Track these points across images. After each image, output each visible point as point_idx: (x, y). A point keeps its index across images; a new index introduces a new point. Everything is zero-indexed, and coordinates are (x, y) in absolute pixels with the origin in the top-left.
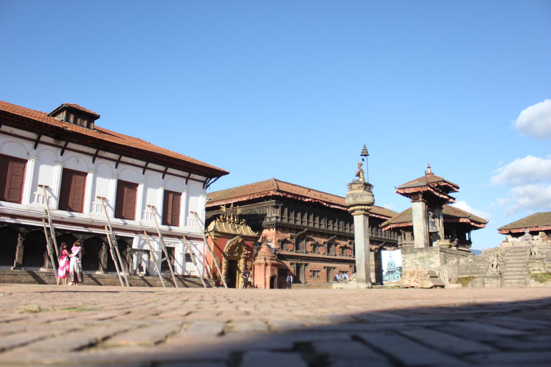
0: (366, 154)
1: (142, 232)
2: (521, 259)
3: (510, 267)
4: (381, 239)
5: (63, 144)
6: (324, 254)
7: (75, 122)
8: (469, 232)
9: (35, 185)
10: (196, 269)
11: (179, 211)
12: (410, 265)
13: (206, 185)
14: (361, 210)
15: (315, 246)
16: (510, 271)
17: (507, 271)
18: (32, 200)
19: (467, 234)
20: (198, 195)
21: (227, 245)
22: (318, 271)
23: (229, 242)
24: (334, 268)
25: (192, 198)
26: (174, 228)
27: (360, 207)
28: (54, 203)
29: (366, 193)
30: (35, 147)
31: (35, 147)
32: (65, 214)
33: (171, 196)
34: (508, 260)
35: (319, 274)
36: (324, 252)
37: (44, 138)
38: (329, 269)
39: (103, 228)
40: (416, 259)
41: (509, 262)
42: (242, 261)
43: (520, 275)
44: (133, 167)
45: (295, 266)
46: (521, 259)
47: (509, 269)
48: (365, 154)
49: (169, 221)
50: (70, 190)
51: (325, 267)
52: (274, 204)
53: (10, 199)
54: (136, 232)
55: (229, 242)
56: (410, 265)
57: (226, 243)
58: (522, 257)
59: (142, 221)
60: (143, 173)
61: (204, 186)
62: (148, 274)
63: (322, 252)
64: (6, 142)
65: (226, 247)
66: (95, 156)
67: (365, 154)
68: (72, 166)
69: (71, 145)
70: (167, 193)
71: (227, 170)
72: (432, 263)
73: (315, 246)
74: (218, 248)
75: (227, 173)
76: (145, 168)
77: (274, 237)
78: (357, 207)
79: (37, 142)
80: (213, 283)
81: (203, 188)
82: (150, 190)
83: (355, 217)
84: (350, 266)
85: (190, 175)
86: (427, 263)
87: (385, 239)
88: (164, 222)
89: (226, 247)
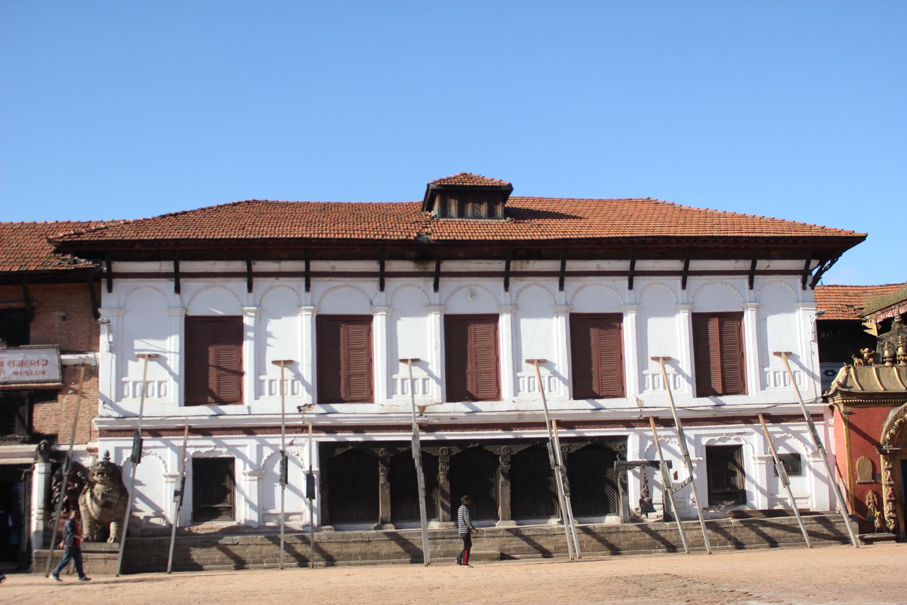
1: (645, 422)
5: (431, 267)
7: (461, 214)
9: (393, 362)
10: (811, 491)
11: (742, 356)
13: (810, 279)
18: (391, 391)
20: (790, 309)
25: (773, 321)
26: (731, 402)
28: (436, 391)
30: (382, 287)
31: (382, 287)
32: (459, 409)
33: (713, 326)
37: (393, 266)
39: (542, 425)
44: (602, 278)
49: (717, 385)
50: (466, 357)
53: (353, 397)
54: (628, 423)
59: (641, 397)
60: (631, 287)
61: (804, 282)
62: (668, 517)
64: (329, 290)
66: (507, 276)
68: (462, 306)
69: (448, 266)
70: (699, 322)
71: (859, 232)
74: (860, 435)
75: (862, 239)
76: (631, 275)
79: (382, 277)
80: (850, 528)
81: (804, 288)
82: (654, 324)
85: (754, 264)
88: (703, 388)
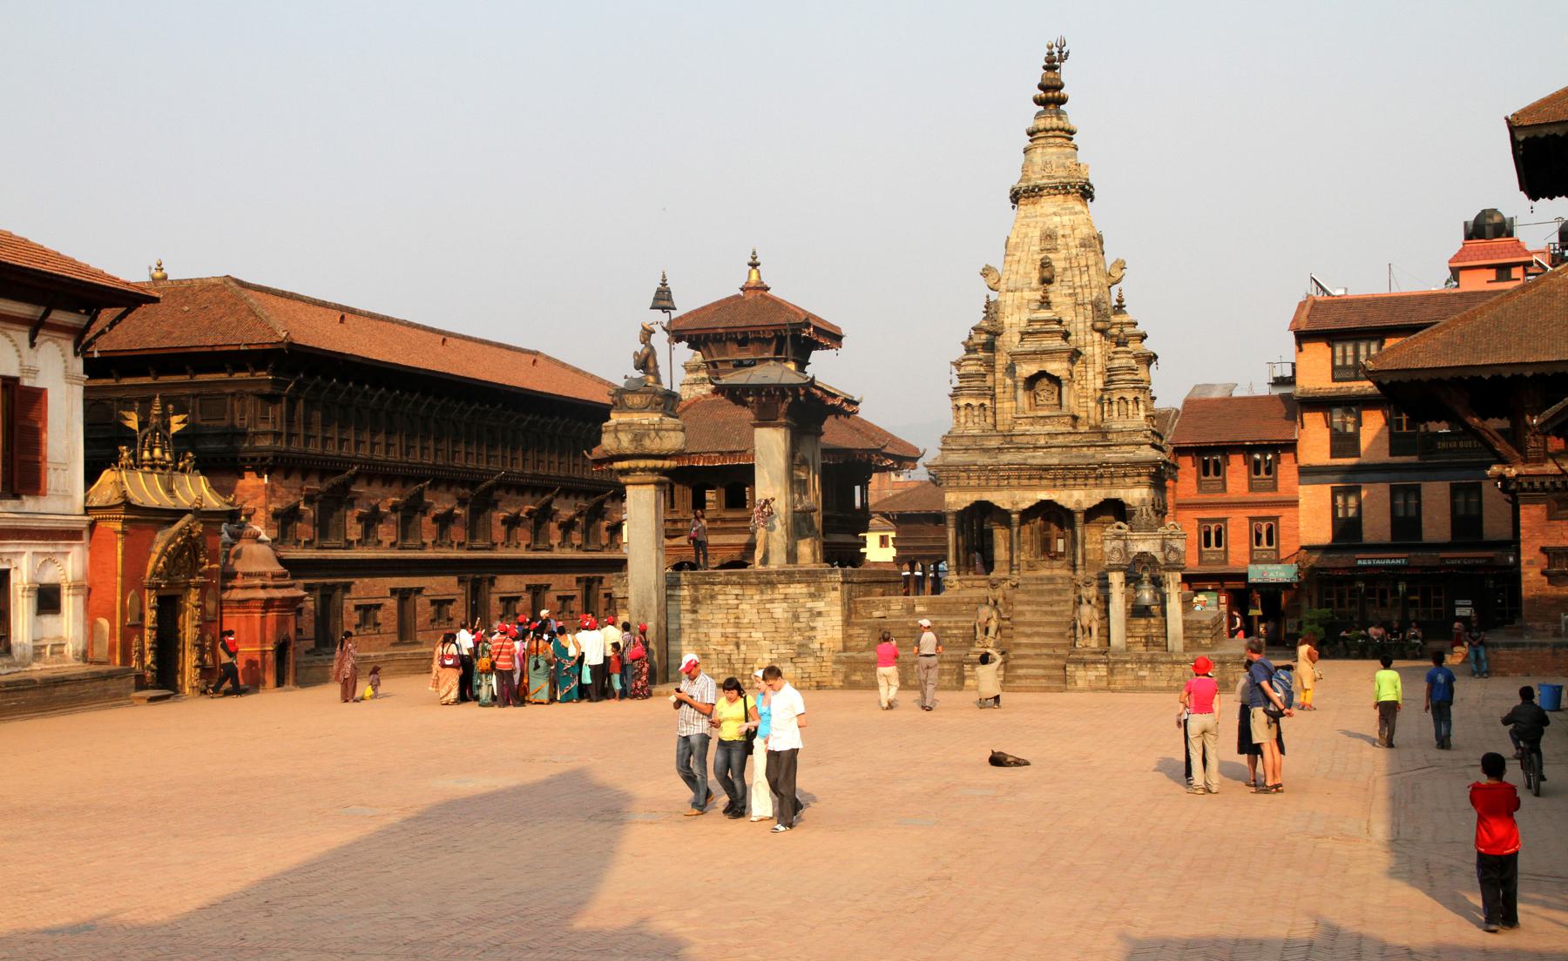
0: (665, 303)
2: (1054, 613)
3: (1028, 636)
4: (547, 477)
6: (393, 545)
8: (865, 486)
12: (755, 618)
14: (653, 470)
15: (371, 520)
16: (1027, 645)
17: (1018, 645)
19: (857, 488)
21: (158, 549)
22: (378, 607)
23: (161, 541)
24: (419, 591)
27: (651, 463)
29: (669, 422)
34: (1021, 613)
35: (380, 615)
36: (393, 539)
38: (403, 595)
40: (772, 601)
41: (1021, 619)
42: (193, 597)
43: (1049, 656)
45: (318, 593)
46: (1054, 613)
47: (1024, 640)
51: (394, 591)
52: (267, 389)
55: (161, 541)
56: (755, 618)
57: (151, 542)
58: (1055, 608)
63: (386, 543)
65: (154, 557)
72: (820, 614)
73: (371, 520)
77: (261, 500)
78: (642, 463)
83: (630, 490)
84: (461, 581)
85: (47, 314)
86: (804, 617)
87: (559, 479)
89: (154, 557)
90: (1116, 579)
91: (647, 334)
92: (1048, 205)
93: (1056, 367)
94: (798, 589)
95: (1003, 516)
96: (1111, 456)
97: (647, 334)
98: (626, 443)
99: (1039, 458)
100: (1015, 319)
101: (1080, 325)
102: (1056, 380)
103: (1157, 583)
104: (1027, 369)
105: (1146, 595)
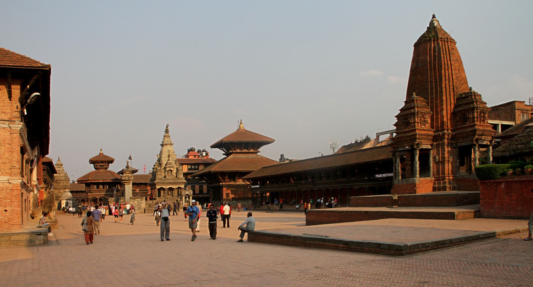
48: (130, 158)
67: (130, 158)
90: (184, 197)
91: (128, 162)
92: (168, 146)
93: (171, 169)
94: (139, 199)
95: (164, 189)
96: (180, 181)
97: (128, 162)
98: (127, 178)
99: (170, 181)
100: (164, 162)
101: (174, 163)
102: (171, 171)
103: (189, 198)
104: (168, 169)
105: (187, 199)
